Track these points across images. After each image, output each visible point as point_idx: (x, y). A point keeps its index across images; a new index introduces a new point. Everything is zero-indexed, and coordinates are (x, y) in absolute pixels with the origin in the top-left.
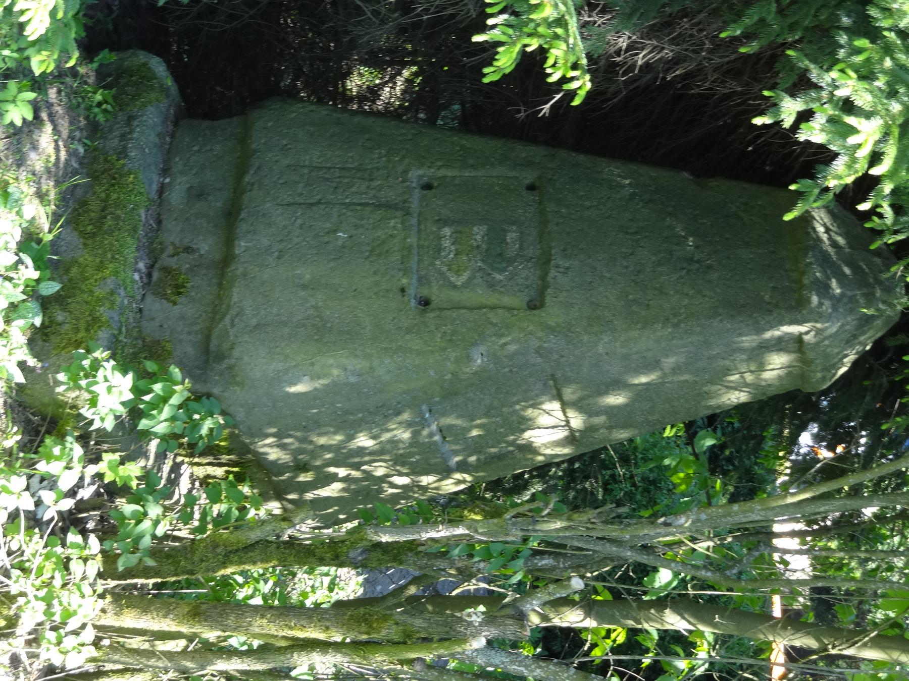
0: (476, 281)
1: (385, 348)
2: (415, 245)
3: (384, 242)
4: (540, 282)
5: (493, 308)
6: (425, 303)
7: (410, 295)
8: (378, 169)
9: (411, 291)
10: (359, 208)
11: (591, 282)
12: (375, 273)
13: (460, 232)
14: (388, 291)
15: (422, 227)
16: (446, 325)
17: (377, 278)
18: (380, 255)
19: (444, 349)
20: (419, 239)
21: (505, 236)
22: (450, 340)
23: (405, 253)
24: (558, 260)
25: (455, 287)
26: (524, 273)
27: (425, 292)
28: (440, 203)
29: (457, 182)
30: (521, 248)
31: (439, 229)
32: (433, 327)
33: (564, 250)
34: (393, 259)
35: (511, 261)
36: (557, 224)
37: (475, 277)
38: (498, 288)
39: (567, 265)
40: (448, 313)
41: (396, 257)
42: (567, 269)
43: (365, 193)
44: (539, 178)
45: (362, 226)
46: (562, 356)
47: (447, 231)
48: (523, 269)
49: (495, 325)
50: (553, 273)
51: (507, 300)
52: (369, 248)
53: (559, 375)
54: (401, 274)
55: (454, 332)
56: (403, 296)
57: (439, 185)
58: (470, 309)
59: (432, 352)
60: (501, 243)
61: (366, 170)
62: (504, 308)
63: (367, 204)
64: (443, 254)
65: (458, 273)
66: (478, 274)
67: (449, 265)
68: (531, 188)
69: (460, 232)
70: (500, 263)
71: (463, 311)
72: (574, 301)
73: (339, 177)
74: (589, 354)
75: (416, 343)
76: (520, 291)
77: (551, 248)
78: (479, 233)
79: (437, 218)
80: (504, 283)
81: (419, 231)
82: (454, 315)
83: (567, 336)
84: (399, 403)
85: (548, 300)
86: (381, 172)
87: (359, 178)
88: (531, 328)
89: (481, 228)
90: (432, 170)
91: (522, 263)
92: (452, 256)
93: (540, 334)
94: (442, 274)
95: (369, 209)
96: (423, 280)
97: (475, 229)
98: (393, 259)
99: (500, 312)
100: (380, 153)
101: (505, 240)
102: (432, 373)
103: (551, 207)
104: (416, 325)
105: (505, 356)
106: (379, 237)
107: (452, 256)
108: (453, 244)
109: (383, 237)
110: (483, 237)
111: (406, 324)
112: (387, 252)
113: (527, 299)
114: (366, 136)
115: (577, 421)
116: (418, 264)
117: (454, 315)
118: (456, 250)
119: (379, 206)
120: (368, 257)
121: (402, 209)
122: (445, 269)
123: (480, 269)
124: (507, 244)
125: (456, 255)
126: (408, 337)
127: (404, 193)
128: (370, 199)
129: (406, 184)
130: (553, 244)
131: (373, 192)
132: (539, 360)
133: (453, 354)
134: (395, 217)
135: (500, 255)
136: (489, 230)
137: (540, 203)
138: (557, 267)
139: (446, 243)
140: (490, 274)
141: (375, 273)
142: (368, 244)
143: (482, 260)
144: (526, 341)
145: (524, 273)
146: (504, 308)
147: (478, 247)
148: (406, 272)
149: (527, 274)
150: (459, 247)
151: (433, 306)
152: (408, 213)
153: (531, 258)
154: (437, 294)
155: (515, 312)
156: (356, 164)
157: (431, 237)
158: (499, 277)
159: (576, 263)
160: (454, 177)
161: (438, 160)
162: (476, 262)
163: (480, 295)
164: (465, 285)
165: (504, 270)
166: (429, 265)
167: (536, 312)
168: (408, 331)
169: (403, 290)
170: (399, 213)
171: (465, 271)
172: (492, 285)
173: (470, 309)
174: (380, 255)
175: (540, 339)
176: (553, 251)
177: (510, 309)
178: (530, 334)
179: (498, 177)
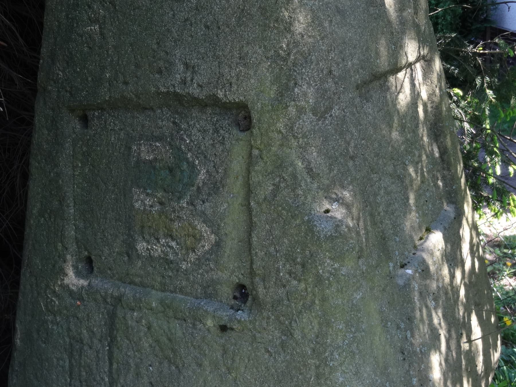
0: (209, 212)
1: (318, 376)
2: (160, 294)
3: (157, 341)
4: (209, 110)
5: (249, 191)
6: (243, 294)
7: (231, 320)
8: (69, 330)
9: (225, 315)
10: (115, 366)
11: (207, 27)
12: (200, 365)
13: (143, 227)
14: (225, 352)
15: (137, 280)
16: (278, 271)
17: (206, 363)
18: (174, 351)
19: (319, 280)
20: (153, 287)
21: (145, 162)
22: (303, 266)
23: (171, 314)
24: (174, 81)
25: (218, 245)
26: (197, 135)
27: (226, 292)
28: (106, 251)
29: (81, 225)
30: (159, 139)
31: (139, 256)
32: (281, 291)
33: (160, 72)
34: (179, 334)
35: (179, 155)
36: (126, 83)
37: (203, 212)
38: (218, 177)
39: (182, 68)
40: (258, 264)
41: (177, 329)
42: (187, 66)
43: (98, 352)
44: (72, 110)
45: (137, 366)
46: (330, 72)
47: (141, 246)
48: (189, 136)
49: (277, 187)
50: (194, 91)
51: (237, 165)
52: (166, 364)
53: (357, 78)
54: (200, 326)
55: (290, 258)
56: (232, 329)
57: (86, 250)
58: (251, 226)
59: (324, 299)
60: (154, 168)
61: (71, 345)
62: (249, 172)
63: (111, 354)
64: (171, 257)
65: (198, 238)
66: (199, 207)
67: (187, 249)
68: (85, 120)
69: (143, 227)
70: (182, 171)
71: (255, 239)
72: (236, 54)
73: (81, 382)
74: (326, 24)
75: (308, 325)
76: (223, 143)
77: (159, 93)
78: (143, 201)
79: (126, 258)
80: (211, 169)
81: (142, 285)
82: (261, 254)
83: (294, 64)
84: (398, 328)
85: (234, 96)
86: (72, 327)
87: (80, 356)
88: (280, 126)
89: (136, 197)
90: (69, 257)
91: (182, 139)
92: (173, 244)
93: (292, 111)
94: (199, 263)
95: (116, 351)
96: (209, 292)
97: (137, 205)
98: (179, 334)
99: (255, 178)
100: (52, 322)
101: (150, 161)
102: (358, 296)
103: (104, 94)
104: (277, 318)
105: (331, 170)
106: (151, 346)
107: (173, 244)
108: (158, 239)
109: (150, 340)
110: (148, 195)
111: (277, 333)
112: (170, 340)
113: (235, 131)
114: (35, 336)
115: (411, 50)
116: (186, 294)
117: (261, 254)
118: (166, 236)
119: (113, 341)
120: (177, 367)
121: (115, 307)
122: (192, 257)
123: (191, 203)
124: (155, 159)
125: (173, 239)
126: (298, 335)
127: (95, 300)
128: (103, 346)
129: (85, 296)
130: (153, 89)
131: (96, 341)
132: (336, 111)
133: (327, 265)
134: (124, 318)
135: (171, 170)
136: (139, 187)
137: (103, 109)
138: (184, 82)
139: (158, 250)
140: (199, 188)
141: (200, 365)
142: (160, 363)
143: (179, 198)
144: (304, 136)
145: (197, 135)
146: (249, 172)
147: (161, 203)
148: (197, 318)
149: (197, 130)
150: (161, 233)
151: (246, 282)
152: (119, 299)
153: (174, 123)
154: (228, 273)
155: (256, 152)
156: (65, 356)
157: (149, 269)
158: (202, 176)
159: (178, 52)
160: (77, 228)
161: (56, 249)
162: (182, 208)
163: (230, 206)
164: (216, 230)
165: (192, 166)
166: (188, 279)
167: (255, 116)
168: (288, 332)
169: (224, 328)
170: (120, 313)
171: (194, 228)
172: (216, 187)
173: (251, 226)
174: (174, 351)
175: (301, 111)
176: (163, 90)
177: (250, 162)
178: (292, 128)
179: (74, 168)
